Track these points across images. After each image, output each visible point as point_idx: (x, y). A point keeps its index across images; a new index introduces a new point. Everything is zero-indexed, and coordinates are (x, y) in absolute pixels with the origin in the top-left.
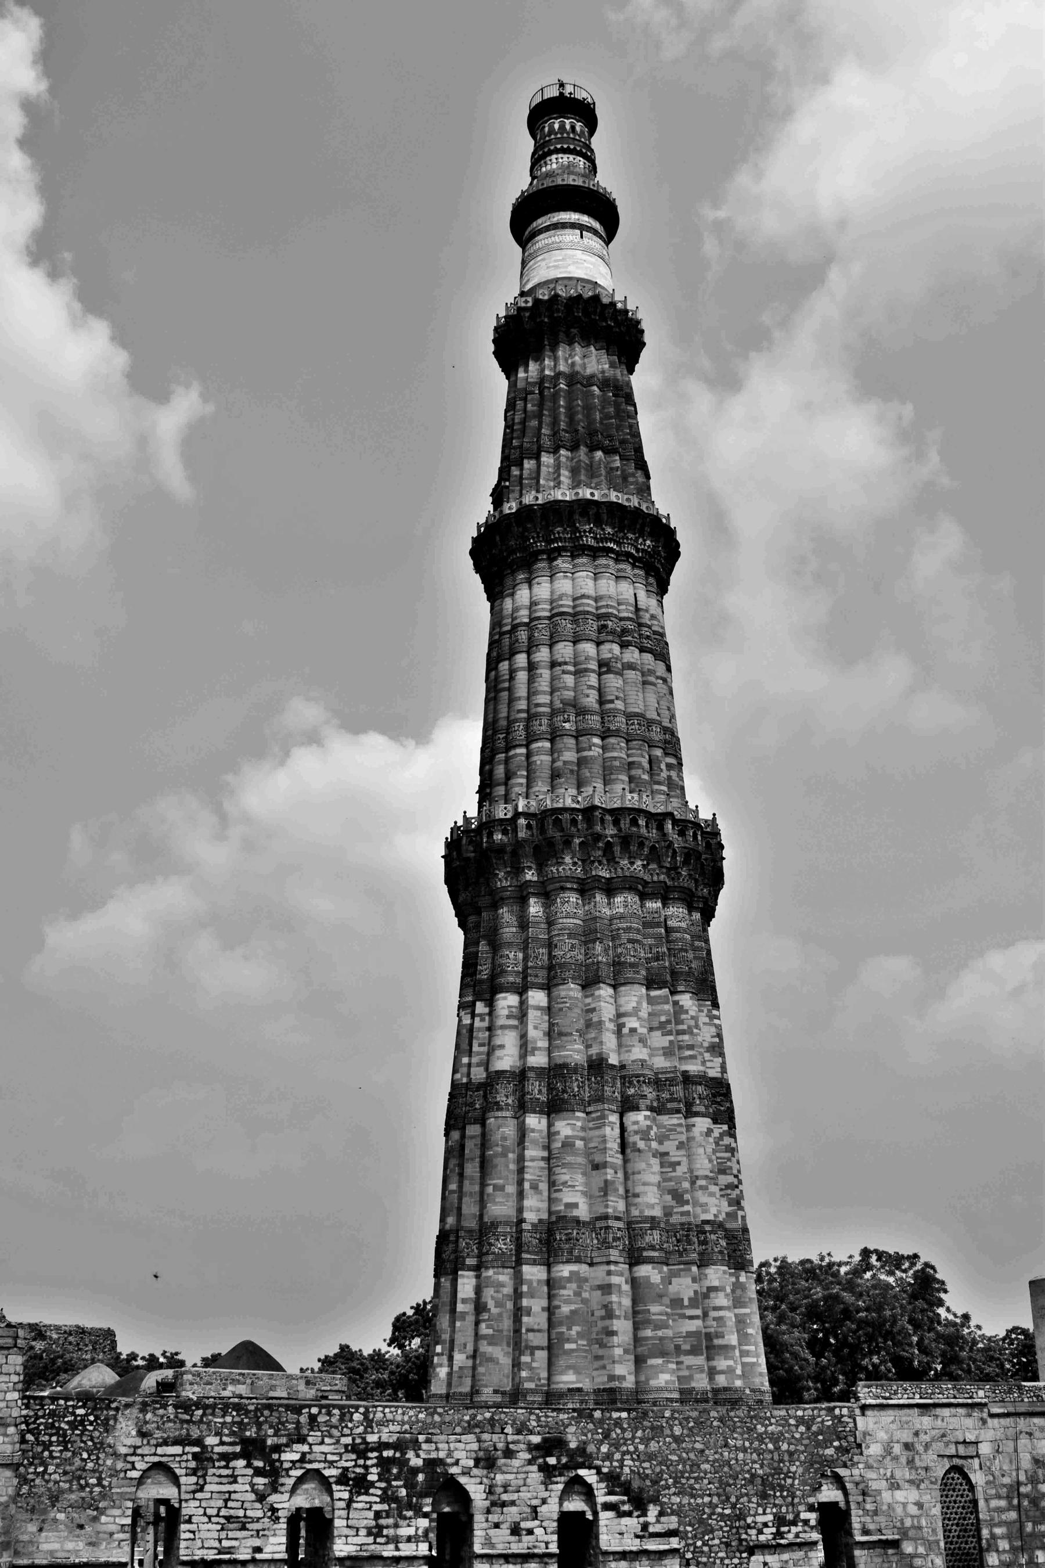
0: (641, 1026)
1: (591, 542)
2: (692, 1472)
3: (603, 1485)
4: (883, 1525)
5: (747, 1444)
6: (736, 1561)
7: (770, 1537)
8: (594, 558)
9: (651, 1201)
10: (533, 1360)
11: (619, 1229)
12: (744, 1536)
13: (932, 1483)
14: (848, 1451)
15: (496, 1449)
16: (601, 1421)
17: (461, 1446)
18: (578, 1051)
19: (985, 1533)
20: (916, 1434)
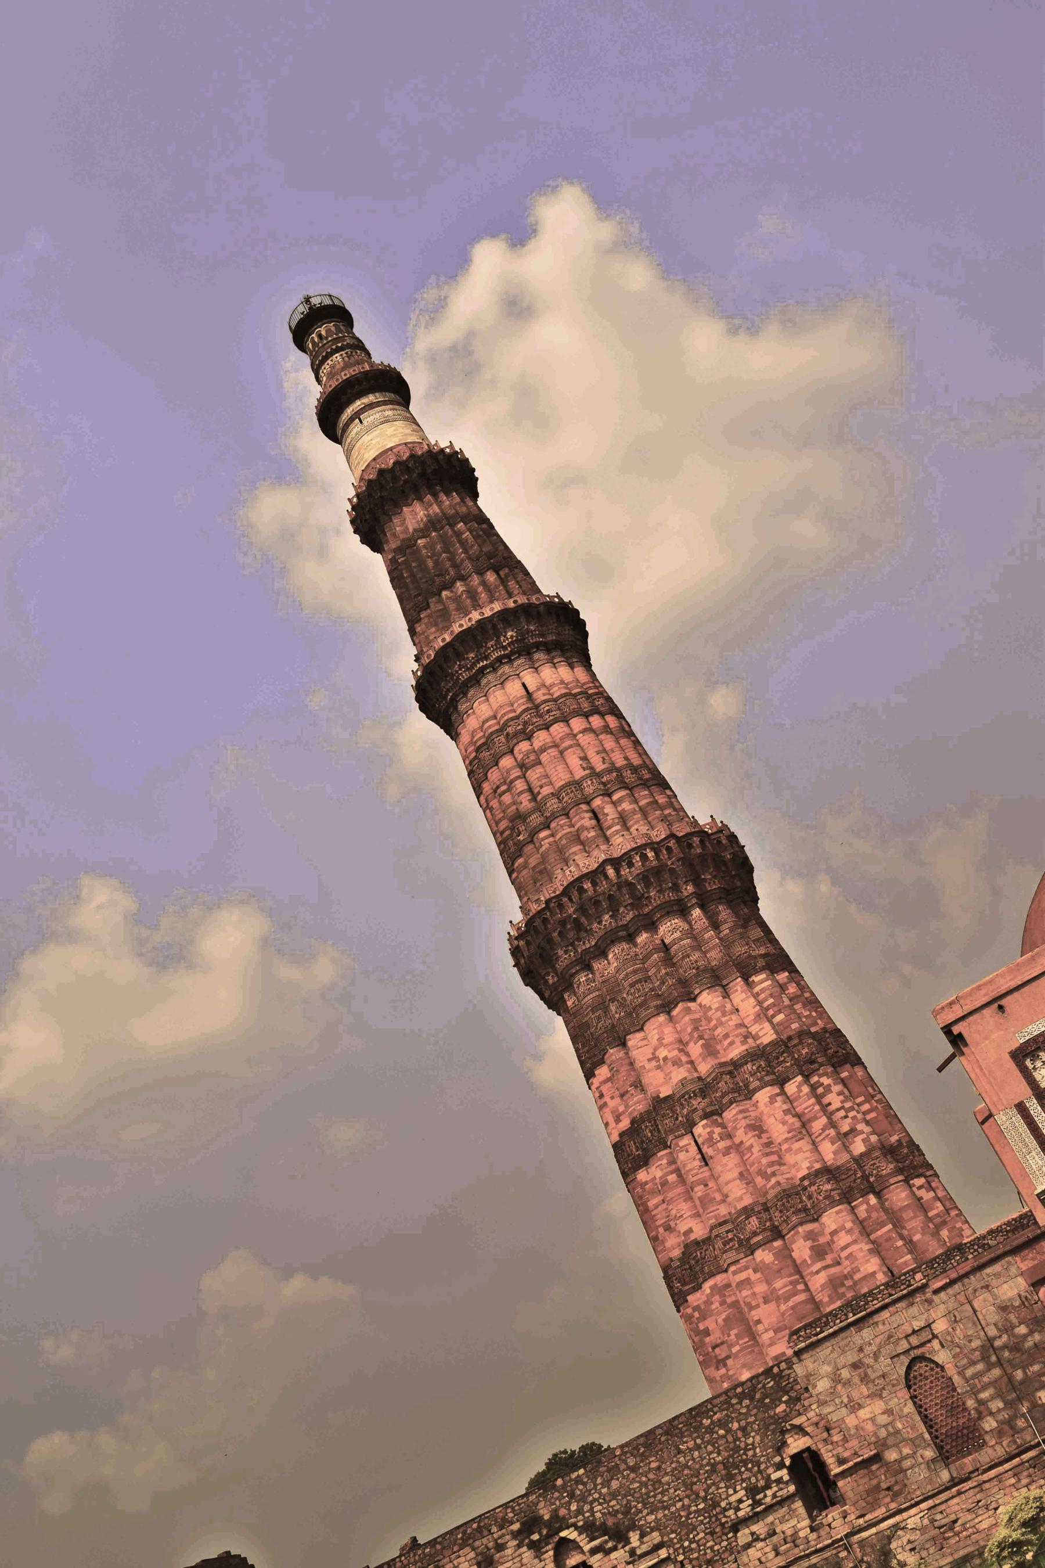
1: (466, 675)
2: (655, 1489)
3: (584, 1536)
5: (699, 1441)
6: (725, 1543)
8: (478, 683)
9: (740, 1196)
10: (728, 1370)
11: (727, 1232)
12: (724, 1520)
13: (893, 1386)
14: (798, 1399)
15: (489, 1549)
16: (564, 1486)
17: (462, 1559)
18: (639, 1102)
19: (970, 1403)
20: (861, 1350)
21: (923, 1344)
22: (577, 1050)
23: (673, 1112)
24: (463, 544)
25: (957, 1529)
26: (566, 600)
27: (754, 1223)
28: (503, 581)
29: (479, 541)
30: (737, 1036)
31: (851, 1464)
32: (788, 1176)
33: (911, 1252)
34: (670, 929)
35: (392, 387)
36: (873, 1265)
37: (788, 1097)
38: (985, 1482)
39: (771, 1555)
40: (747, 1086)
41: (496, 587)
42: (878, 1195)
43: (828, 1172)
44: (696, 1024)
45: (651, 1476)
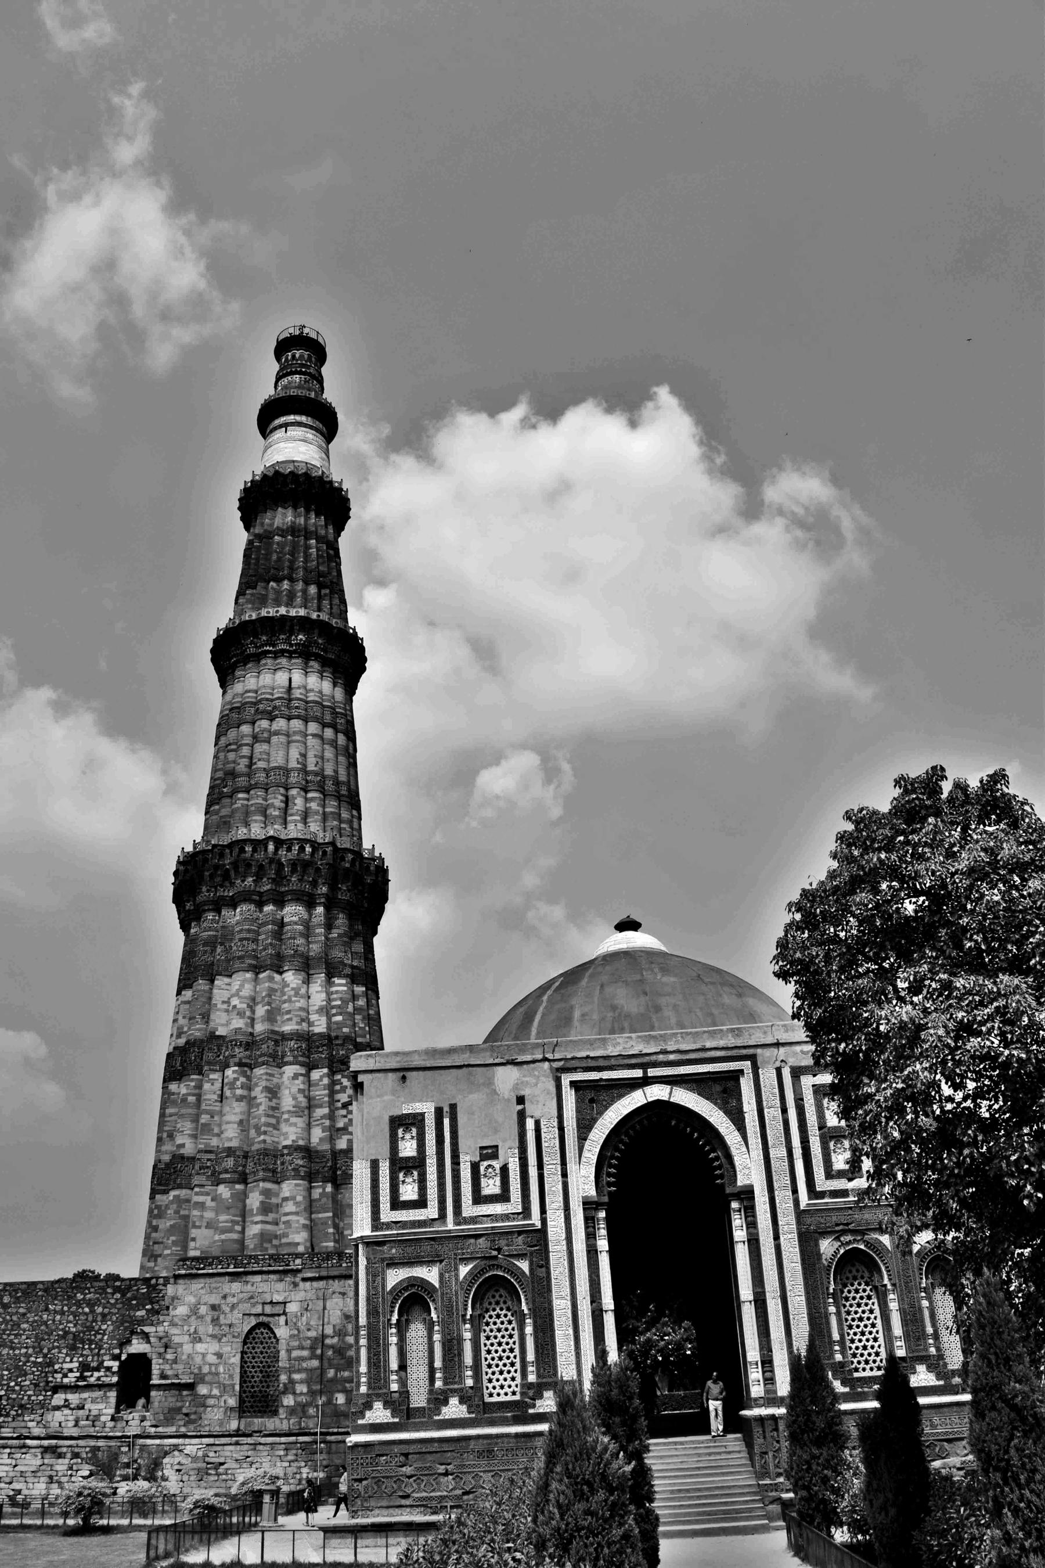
0: (241, 1003)
1: (252, 650)
2: (12, 1330)
4: (180, 1372)
5: (66, 1308)
6: (41, 1398)
7: (74, 1380)
8: (259, 661)
9: (231, 1136)
11: (208, 1160)
12: (50, 1379)
13: (234, 1337)
14: (158, 1313)
18: (199, 1030)
19: (283, 1378)
20: (225, 1297)
21: (273, 1315)
22: (181, 969)
23: (219, 1050)
24: (307, 556)
25: (221, 1470)
26: (360, 635)
27: (230, 1163)
28: (320, 598)
29: (320, 560)
30: (297, 1016)
31: (169, 1381)
32: (276, 1140)
33: (336, 1241)
34: (293, 912)
35: (326, 422)
36: (299, 1238)
37: (309, 1081)
38: (260, 1444)
39: (71, 1424)
40: (283, 1057)
41: (313, 599)
42: (337, 1186)
43: (307, 1151)
44: (271, 991)
45: (15, 1318)
